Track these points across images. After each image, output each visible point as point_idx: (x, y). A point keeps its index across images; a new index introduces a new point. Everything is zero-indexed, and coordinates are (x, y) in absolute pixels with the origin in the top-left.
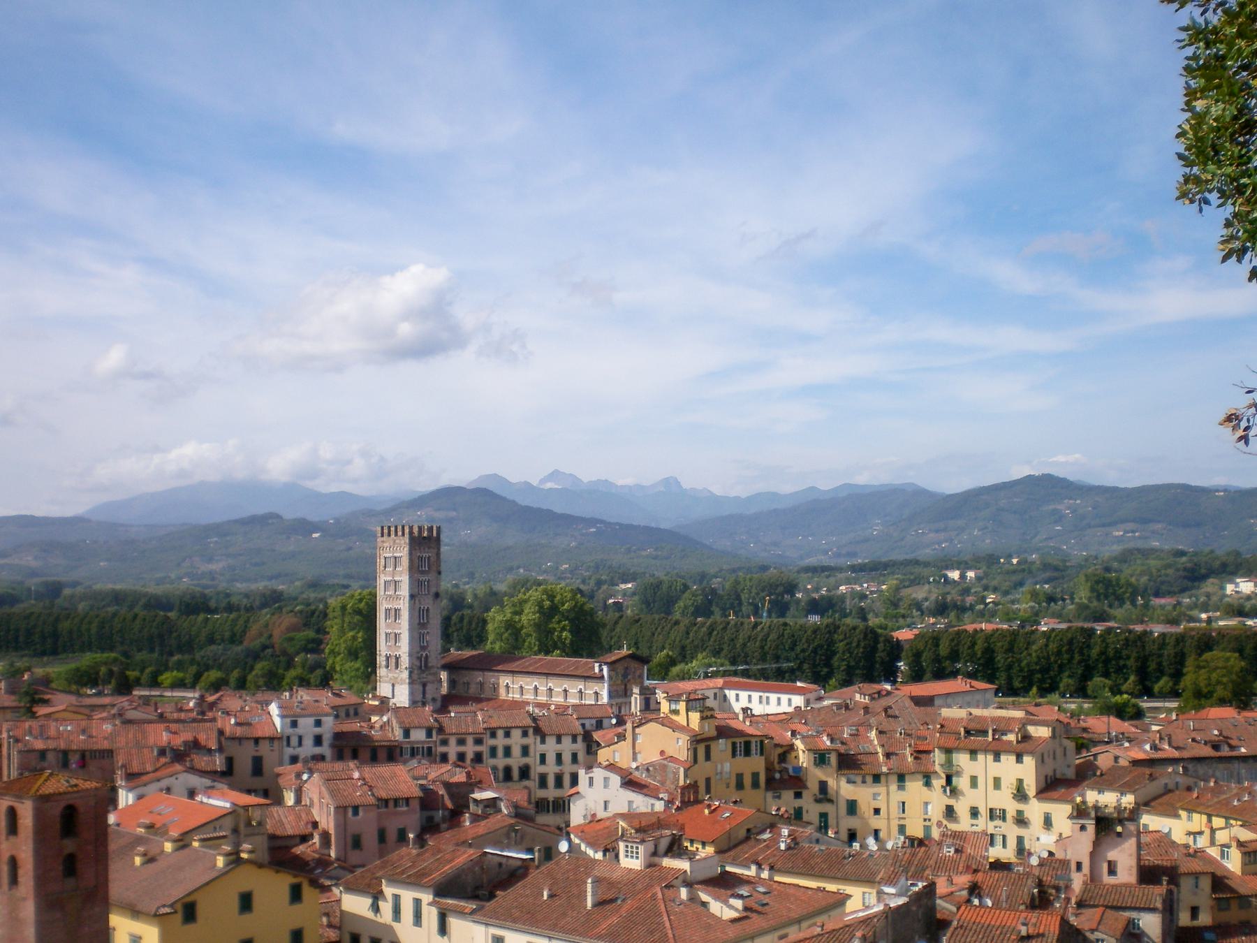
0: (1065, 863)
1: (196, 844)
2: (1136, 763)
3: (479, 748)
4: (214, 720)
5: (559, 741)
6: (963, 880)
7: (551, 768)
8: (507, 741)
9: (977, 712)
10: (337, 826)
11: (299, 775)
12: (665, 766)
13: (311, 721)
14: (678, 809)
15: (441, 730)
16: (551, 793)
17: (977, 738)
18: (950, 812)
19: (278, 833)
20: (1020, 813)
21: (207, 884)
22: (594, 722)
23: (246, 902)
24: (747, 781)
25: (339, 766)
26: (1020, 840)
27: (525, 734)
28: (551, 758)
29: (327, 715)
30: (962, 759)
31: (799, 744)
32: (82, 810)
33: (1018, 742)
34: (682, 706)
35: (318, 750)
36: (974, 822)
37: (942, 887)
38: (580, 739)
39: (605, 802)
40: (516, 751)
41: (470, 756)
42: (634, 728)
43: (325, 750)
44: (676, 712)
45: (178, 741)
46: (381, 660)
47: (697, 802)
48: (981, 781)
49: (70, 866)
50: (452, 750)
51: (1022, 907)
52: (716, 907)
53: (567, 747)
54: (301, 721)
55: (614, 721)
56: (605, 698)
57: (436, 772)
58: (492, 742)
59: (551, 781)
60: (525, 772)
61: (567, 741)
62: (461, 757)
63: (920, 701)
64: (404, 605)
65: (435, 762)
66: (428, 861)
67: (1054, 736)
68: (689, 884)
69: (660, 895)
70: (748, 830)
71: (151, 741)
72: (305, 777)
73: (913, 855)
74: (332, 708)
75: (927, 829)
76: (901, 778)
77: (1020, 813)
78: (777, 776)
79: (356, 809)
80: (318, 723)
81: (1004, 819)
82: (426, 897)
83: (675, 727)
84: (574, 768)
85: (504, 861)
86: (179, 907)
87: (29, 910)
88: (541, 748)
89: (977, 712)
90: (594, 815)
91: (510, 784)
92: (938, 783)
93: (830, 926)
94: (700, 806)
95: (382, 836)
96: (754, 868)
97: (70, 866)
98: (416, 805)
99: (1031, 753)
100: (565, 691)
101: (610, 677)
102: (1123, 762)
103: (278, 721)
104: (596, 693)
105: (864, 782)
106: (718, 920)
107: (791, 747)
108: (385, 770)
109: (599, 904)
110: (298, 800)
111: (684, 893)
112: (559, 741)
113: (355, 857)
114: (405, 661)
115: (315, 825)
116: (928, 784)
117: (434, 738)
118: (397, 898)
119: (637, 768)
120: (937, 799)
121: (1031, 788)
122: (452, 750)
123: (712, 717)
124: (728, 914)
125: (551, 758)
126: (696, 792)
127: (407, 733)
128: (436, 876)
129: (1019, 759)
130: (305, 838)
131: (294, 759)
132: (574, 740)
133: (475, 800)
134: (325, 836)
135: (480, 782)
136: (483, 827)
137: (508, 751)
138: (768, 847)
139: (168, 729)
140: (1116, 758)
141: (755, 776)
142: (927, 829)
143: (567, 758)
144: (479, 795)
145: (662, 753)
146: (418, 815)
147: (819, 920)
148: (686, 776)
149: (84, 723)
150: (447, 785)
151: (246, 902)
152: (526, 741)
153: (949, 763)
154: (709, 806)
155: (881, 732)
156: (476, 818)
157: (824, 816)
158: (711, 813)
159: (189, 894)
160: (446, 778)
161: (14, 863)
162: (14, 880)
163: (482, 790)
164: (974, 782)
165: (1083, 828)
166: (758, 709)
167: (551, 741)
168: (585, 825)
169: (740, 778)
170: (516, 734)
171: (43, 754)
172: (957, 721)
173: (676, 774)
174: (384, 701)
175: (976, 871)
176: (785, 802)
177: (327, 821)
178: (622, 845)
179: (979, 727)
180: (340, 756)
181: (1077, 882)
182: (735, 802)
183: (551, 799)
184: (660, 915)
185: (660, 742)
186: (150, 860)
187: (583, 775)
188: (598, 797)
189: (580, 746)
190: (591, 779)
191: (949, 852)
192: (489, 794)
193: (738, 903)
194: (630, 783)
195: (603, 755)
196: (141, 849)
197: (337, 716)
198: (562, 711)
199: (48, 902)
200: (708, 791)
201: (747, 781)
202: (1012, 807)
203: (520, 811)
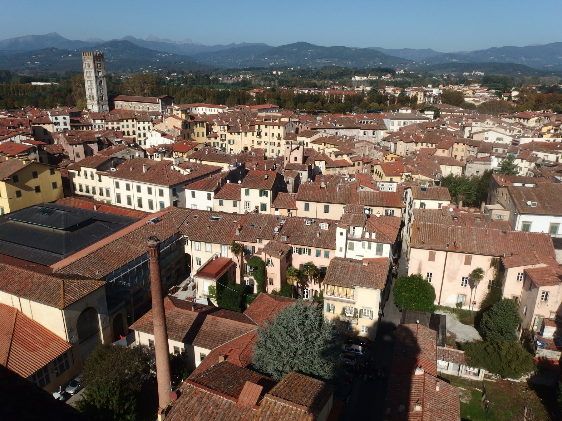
0: (282, 158)
7: (142, 132)
8: (127, 123)
9: (267, 114)
13: (62, 117)
17: (267, 122)
18: (259, 143)
20: (279, 143)
24: (201, 135)
26: (279, 151)
28: (142, 128)
30: (263, 127)
34: (179, 112)
35: (65, 127)
40: (131, 126)
41: (116, 127)
44: (178, 114)
46: (88, 97)
48: (268, 134)
54: (58, 117)
56: (160, 110)
59: (142, 135)
60: (134, 133)
64: (93, 80)
76: (246, 133)
77: (279, 143)
80: (64, 118)
82: (95, 171)
83: (178, 118)
88: (138, 125)
92: (256, 134)
102: (309, 129)
116: (253, 135)
118: (85, 172)
120: (255, 138)
121: (282, 136)
129: (279, 128)
137: (128, 126)
141: (203, 133)
143: (147, 128)
148: (181, 133)
153: (259, 128)
159: (15, 173)
164: (266, 134)
165: (288, 148)
166: (208, 113)
169: (198, 133)
173: (178, 133)
176: (212, 140)
178: (154, 154)
181: (286, 162)
187: (148, 134)
189: (151, 124)
191: (253, 154)
193: (189, 170)
195: (157, 126)
198: (144, 113)
201: (201, 135)
202: (277, 141)
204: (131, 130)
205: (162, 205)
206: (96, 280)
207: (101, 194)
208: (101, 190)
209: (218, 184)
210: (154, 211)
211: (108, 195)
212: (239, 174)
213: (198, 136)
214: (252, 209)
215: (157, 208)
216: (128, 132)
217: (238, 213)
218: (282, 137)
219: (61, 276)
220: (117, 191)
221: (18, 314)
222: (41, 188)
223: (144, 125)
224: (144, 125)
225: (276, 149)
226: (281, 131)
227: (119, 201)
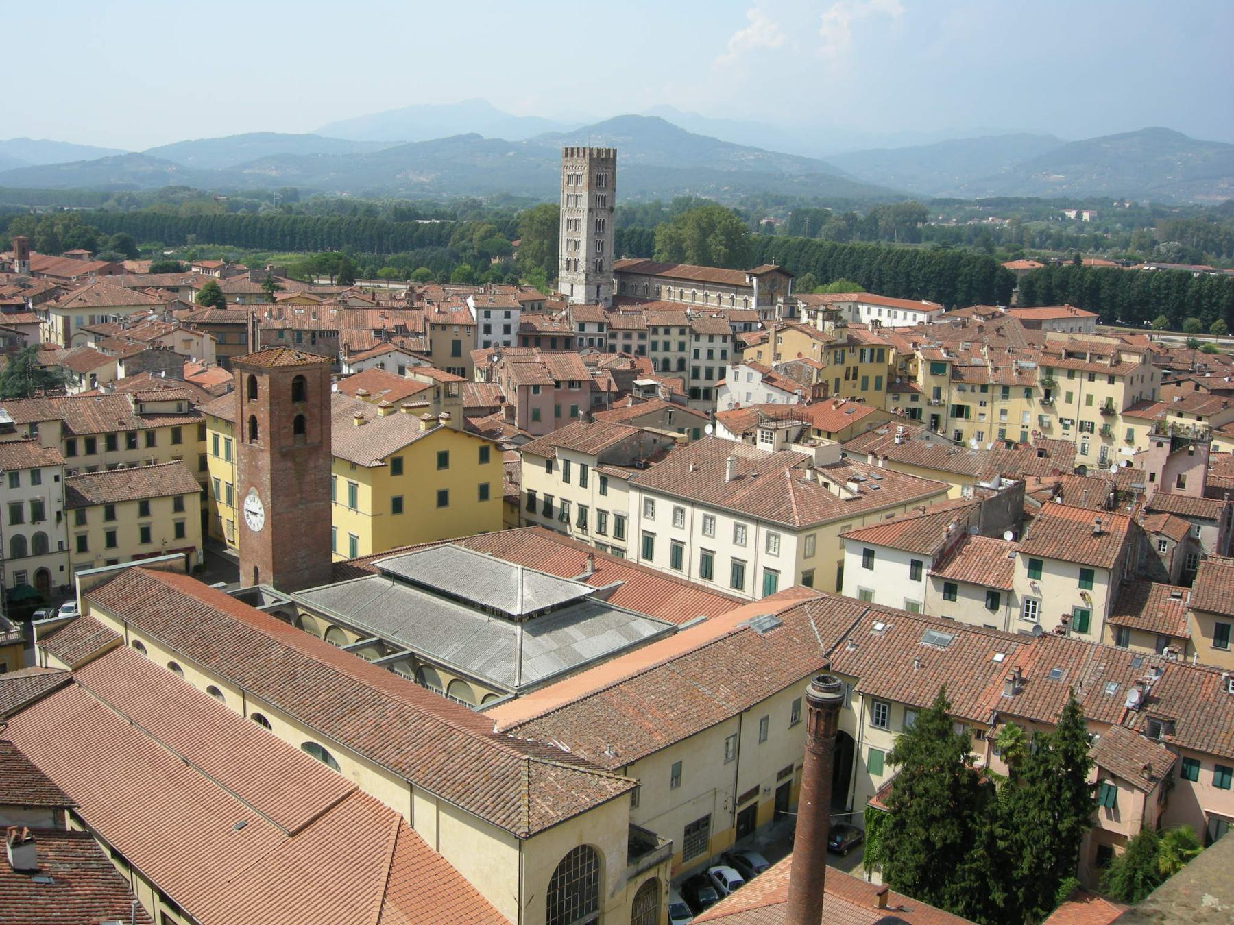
1: (403, 411)
2: (1214, 392)
3: (642, 342)
4: (421, 308)
5: (711, 340)
6: (1049, 480)
7: (703, 363)
8: (667, 338)
10: (520, 402)
11: (490, 358)
12: (801, 366)
13: (502, 313)
14: (809, 403)
15: (609, 325)
16: (702, 383)
17: (1076, 361)
19: (472, 405)
21: (412, 444)
22: (742, 325)
23: (443, 460)
24: (872, 383)
25: (523, 351)
27: (682, 332)
28: (703, 354)
31: (919, 354)
32: (309, 379)
33: (1112, 366)
35: (507, 338)
36: (1066, 431)
37: (1031, 485)
38: (729, 339)
40: (674, 346)
41: (634, 348)
42: (776, 332)
43: (513, 337)
45: (391, 326)
46: (562, 263)
47: (826, 398)
49: (300, 425)
50: (620, 342)
51: (1098, 509)
52: (834, 489)
53: (718, 345)
54: (493, 313)
55: (759, 325)
56: (754, 307)
58: (654, 338)
59: (703, 373)
60: (682, 364)
62: (627, 349)
63: (1028, 324)
64: (583, 217)
66: (594, 432)
67: (1144, 362)
68: (811, 467)
69: (788, 475)
70: (871, 425)
71: (370, 326)
72: (495, 359)
73: (1009, 455)
75: (1024, 434)
78: (898, 381)
79: (536, 388)
80: (507, 315)
81: (1092, 431)
84: (722, 364)
85: (658, 438)
86: (389, 462)
87: (265, 460)
88: (695, 345)
89: (1079, 337)
90: (737, 404)
93: (929, 512)
95: (557, 413)
96: (870, 458)
97: (300, 425)
99: (1122, 377)
100: (719, 297)
101: (759, 287)
103: (473, 312)
104: (746, 301)
105: (973, 391)
106: (836, 499)
107: (912, 356)
108: (560, 356)
109: (738, 478)
110: (489, 379)
111: (808, 474)
112: (711, 340)
113: (535, 427)
114: (583, 265)
115: (502, 399)
119: (776, 367)
122: (620, 342)
123: (845, 326)
124: (845, 495)
125: (703, 354)
126: (826, 390)
127: (582, 326)
128: (600, 447)
130: (494, 410)
131: (487, 345)
132: (724, 340)
133: (637, 386)
134: (510, 409)
135: (642, 371)
136: (643, 409)
137: (667, 347)
138: (884, 440)
139: (383, 315)
140: (1197, 387)
142: (1024, 434)
143: (717, 354)
144: (639, 382)
145: (799, 355)
147: (922, 505)
148: (818, 375)
149: (314, 308)
150: (615, 373)
151: (443, 460)
152: (682, 338)
154: (836, 403)
155: (992, 349)
156: (637, 401)
157: (935, 417)
160: (613, 365)
161: (253, 421)
162: (254, 435)
163: (643, 378)
164: (1069, 398)
166: (886, 322)
167: (704, 341)
169: (865, 379)
170: (675, 332)
171: (281, 332)
172: (1060, 343)
173: (810, 374)
174: (563, 298)
175: (1062, 474)
177: (512, 399)
178: (759, 432)
179: (1078, 350)
180: (525, 341)
183: (702, 389)
184: (788, 493)
185: (800, 346)
186: (363, 421)
188: (742, 388)
189: (729, 346)
190: (737, 374)
192: (648, 382)
193: (854, 487)
194: (768, 380)
195: (749, 354)
196: (359, 413)
197: (523, 310)
199: (280, 454)
200: (837, 390)
201: (872, 383)
202: (1099, 422)
204: (674, 356)
205: (771, 576)
206: (608, 771)
207: (602, 530)
208: (602, 514)
209: (944, 535)
210: (747, 593)
211: (620, 532)
212: (1008, 513)
213: (865, 387)
214: (1050, 622)
215: (754, 584)
216: (666, 363)
217: (1000, 628)
218: (1119, 410)
219: (520, 746)
220: (648, 525)
221: (403, 829)
222: (451, 498)
223: (711, 345)
224: (711, 345)
225: (1095, 444)
226: (1117, 393)
227: (648, 552)
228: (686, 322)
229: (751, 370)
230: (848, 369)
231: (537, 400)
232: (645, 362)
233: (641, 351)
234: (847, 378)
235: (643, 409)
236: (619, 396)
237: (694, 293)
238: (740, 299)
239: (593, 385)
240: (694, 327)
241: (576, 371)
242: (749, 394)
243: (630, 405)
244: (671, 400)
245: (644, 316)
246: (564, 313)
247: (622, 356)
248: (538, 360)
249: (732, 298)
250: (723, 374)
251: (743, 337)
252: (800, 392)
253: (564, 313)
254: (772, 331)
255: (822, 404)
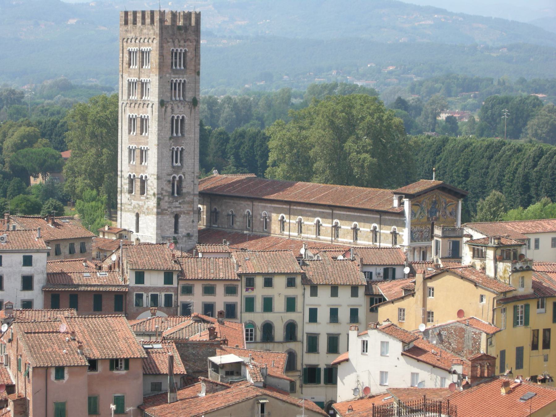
3: (231, 299)
7: (323, 328)
8: (268, 292)
10: (35, 393)
12: (463, 330)
13: (19, 258)
15: (181, 273)
16: (322, 359)
22: (381, 270)
25: (51, 314)
27: (291, 283)
28: (323, 315)
29: (38, 251)
35: (27, 295)
39: (382, 373)
40: (279, 304)
41: (220, 307)
42: (425, 280)
43: (36, 295)
46: (123, 183)
47: (492, 378)
50: (197, 300)
53: (345, 301)
55: (407, 270)
57: (175, 326)
59: (323, 344)
60: (291, 330)
61: (344, 294)
62: (209, 308)
64: (152, 114)
65: (174, 315)
74: (48, 242)
79: (60, 371)
80: (28, 261)
84: (333, 329)
88: (311, 301)
90: (367, 390)
91: (270, 346)
94: (495, 383)
98: (137, 369)
100: (355, 230)
101: (413, 214)
104: (394, 234)
108: (99, 322)
114: (152, 185)
115: (10, 389)
117: (175, 284)
119: (426, 332)
122: (197, 300)
123: (529, 269)
125: (323, 315)
126: (492, 366)
127: (140, 277)
133: (214, 365)
135: (225, 342)
136: (223, 398)
137: (268, 305)
143: (344, 315)
144: (218, 359)
145: (460, 313)
146: (141, 380)
148: (489, 344)
150: (183, 346)
152: (291, 292)
154: (506, 384)
156: (213, 388)
158: (509, 392)
160: (185, 335)
163: (225, 352)
167: (324, 294)
168: (354, 401)
170: (280, 282)
174: (123, 234)
180: (54, 301)
182: (543, 381)
183: (322, 367)
187: (354, 340)
189: (361, 302)
190: (365, 344)
194: (413, 351)
195: (386, 313)
200: (519, 364)
203: (271, 381)
204: (279, 318)
216: (268, 328)
223: (334, 302)
224: (334, 302)
228: (297, 268)
229: (386, 338)
230: (535, 333)
231: (61, 389)
232: (234, 330)
233: (230, 312)
234: (535, 347)
235: (223, 398)
236: (188, 380)
237: (318, 225)
238: (386, 231)
239: (148, 366)
240: (309, 275)
241: (122, 344)
242: (383, 374)
243: (203, 394)
244: (265, 386)
245: (234, 260)
246: (114, 257)
247: (199, 320)
248: (63, 328)
249: (374, 231)
250: (334, 345)
251: (381, 289)
252: (459, 369)
253: (114, 257)
254: (419, 277)
255: (486, 388)
